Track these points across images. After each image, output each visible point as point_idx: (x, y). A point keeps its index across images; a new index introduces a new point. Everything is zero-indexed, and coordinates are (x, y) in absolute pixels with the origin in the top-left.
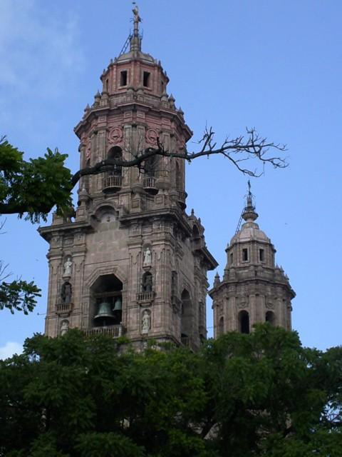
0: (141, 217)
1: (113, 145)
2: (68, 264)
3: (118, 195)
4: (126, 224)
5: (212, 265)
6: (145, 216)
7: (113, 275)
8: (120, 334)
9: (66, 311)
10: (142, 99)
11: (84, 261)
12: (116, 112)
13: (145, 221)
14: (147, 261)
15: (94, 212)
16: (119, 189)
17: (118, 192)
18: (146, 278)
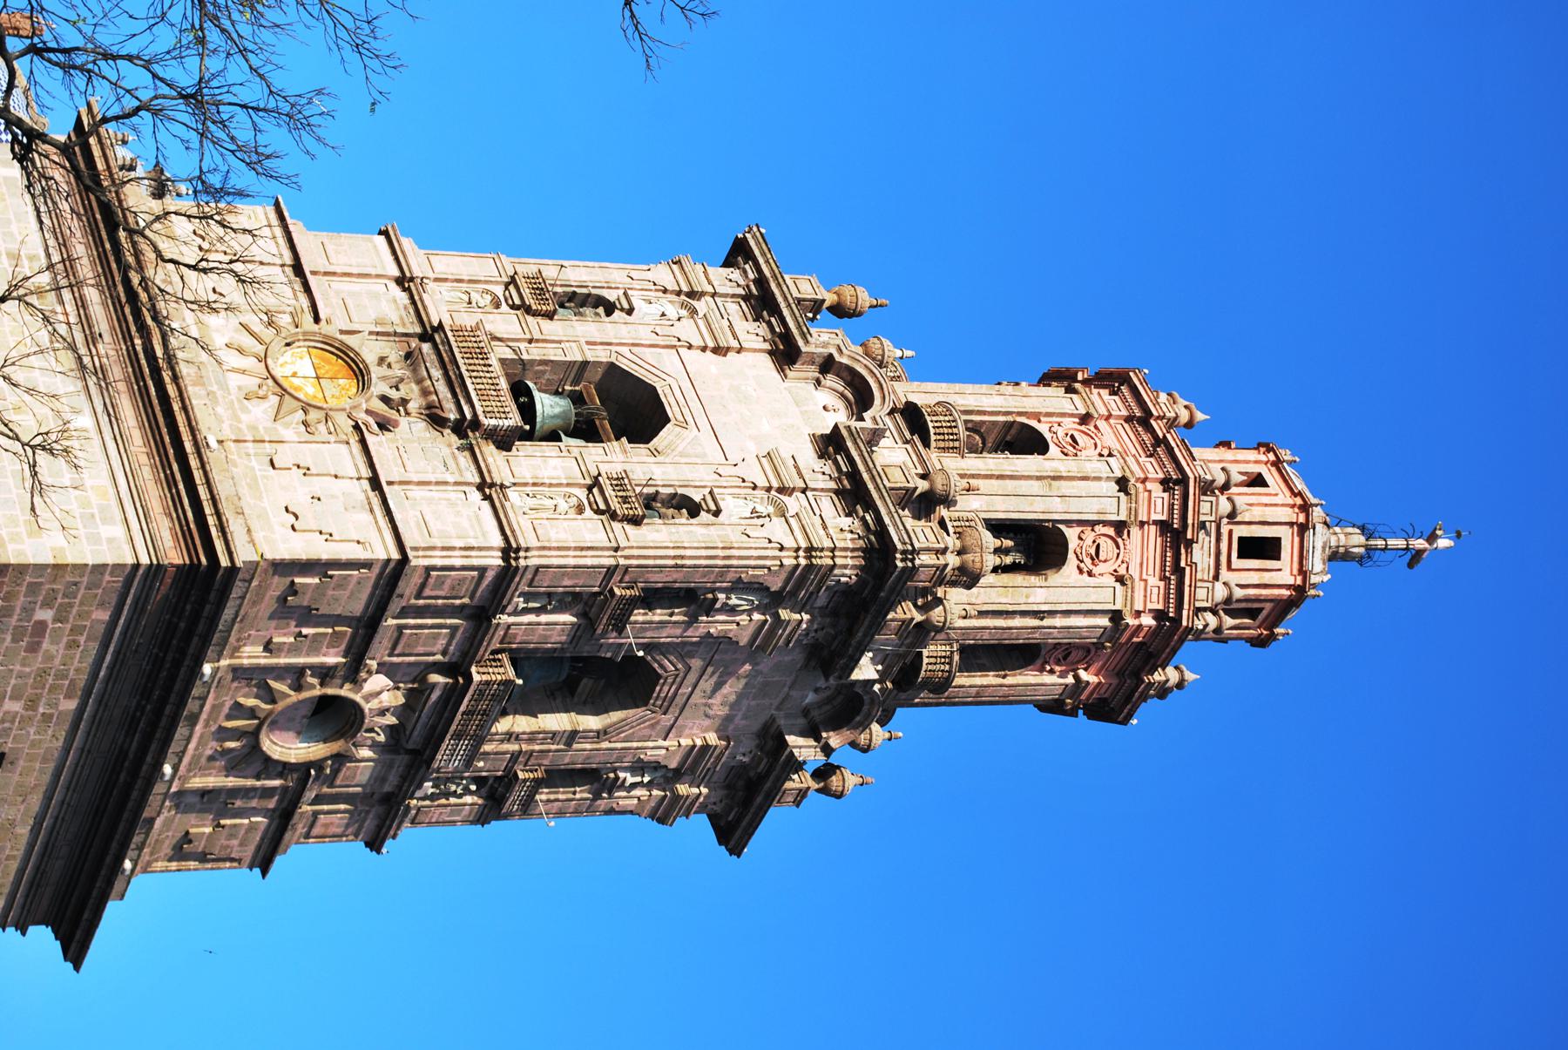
0: (866, 476)
1: (1048, 436)
2: (672, 311)
3: (907, 442)
4: (830, 444)
5: (738, 820)
6: (870, 486)
7: (668, 420)
8: (493, 422)
9: (526, 292)
10: (1205, 507)
11: (690, 347)
12: (1147, 438)
13: (854, 494)
14: (731, 505)
15: (845, 360)
16: (926, 443)
17: (916, 437)
18: (678, 508)
